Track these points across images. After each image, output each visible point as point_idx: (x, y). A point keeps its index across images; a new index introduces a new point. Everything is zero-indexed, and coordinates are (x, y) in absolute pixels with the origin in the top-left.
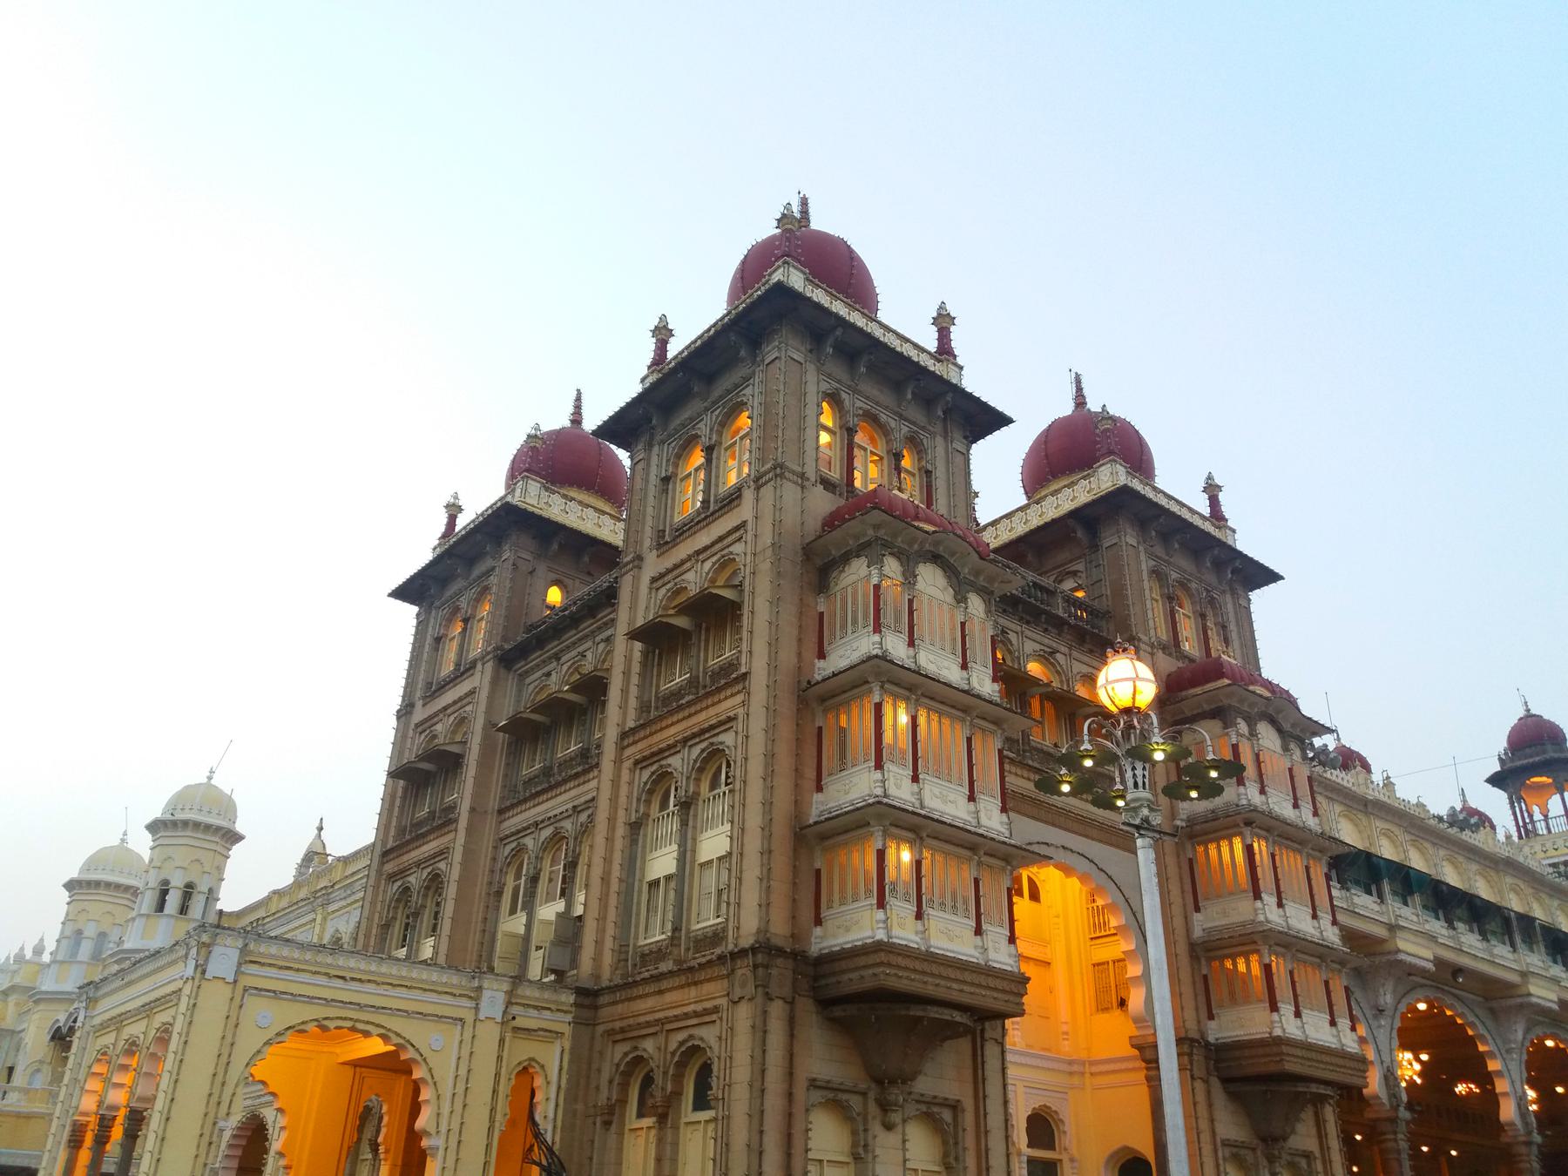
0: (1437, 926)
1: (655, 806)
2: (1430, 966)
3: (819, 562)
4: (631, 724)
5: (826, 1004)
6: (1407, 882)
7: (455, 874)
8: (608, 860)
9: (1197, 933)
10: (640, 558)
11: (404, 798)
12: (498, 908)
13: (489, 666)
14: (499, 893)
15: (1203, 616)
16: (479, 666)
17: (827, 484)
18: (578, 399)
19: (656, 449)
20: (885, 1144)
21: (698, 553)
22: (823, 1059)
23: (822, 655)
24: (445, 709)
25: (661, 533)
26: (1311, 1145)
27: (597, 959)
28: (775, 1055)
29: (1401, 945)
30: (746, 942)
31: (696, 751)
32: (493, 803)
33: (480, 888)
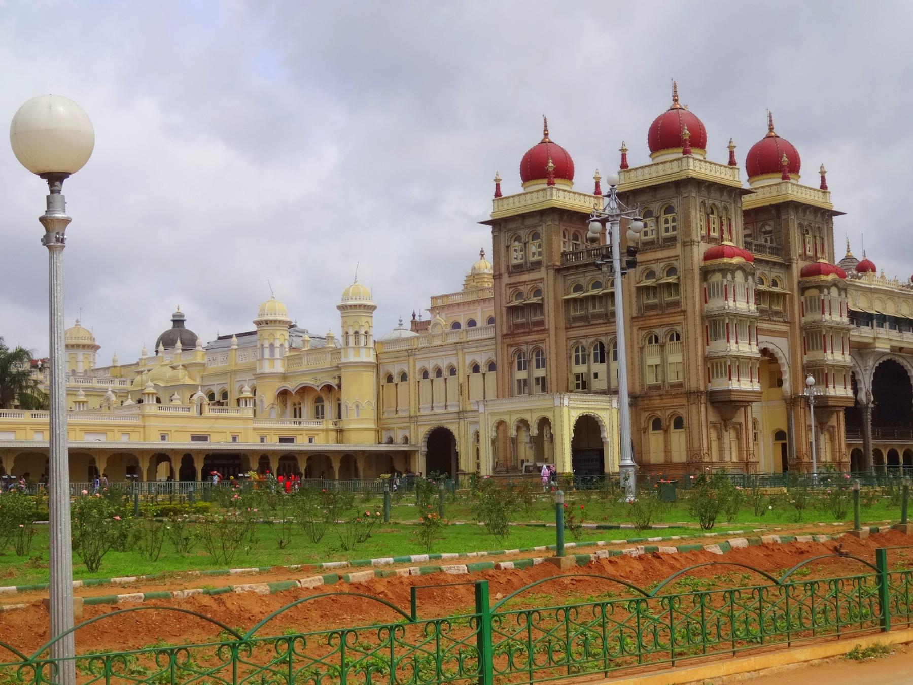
0: (894, 334)
1: (647, 342)
2: (888, 351)
4: (635, 314)
5: (712, 403)
6: (882, 319)
7: (553, 351)
9: (805, 362)
11: (507, 314)
13: (551, 272)
14: (570, 357)
15: (815, 237)
16: (543, 269)
17: (703, 237)
18: (545, 122)
20: (726, 435)
22: (713, 417)
23: (706, 303)
26: (835, 423)
28: (703, 418)
29: (878, 345)
30: (695, 389)
32: (562, 325)
33: (563, 355)
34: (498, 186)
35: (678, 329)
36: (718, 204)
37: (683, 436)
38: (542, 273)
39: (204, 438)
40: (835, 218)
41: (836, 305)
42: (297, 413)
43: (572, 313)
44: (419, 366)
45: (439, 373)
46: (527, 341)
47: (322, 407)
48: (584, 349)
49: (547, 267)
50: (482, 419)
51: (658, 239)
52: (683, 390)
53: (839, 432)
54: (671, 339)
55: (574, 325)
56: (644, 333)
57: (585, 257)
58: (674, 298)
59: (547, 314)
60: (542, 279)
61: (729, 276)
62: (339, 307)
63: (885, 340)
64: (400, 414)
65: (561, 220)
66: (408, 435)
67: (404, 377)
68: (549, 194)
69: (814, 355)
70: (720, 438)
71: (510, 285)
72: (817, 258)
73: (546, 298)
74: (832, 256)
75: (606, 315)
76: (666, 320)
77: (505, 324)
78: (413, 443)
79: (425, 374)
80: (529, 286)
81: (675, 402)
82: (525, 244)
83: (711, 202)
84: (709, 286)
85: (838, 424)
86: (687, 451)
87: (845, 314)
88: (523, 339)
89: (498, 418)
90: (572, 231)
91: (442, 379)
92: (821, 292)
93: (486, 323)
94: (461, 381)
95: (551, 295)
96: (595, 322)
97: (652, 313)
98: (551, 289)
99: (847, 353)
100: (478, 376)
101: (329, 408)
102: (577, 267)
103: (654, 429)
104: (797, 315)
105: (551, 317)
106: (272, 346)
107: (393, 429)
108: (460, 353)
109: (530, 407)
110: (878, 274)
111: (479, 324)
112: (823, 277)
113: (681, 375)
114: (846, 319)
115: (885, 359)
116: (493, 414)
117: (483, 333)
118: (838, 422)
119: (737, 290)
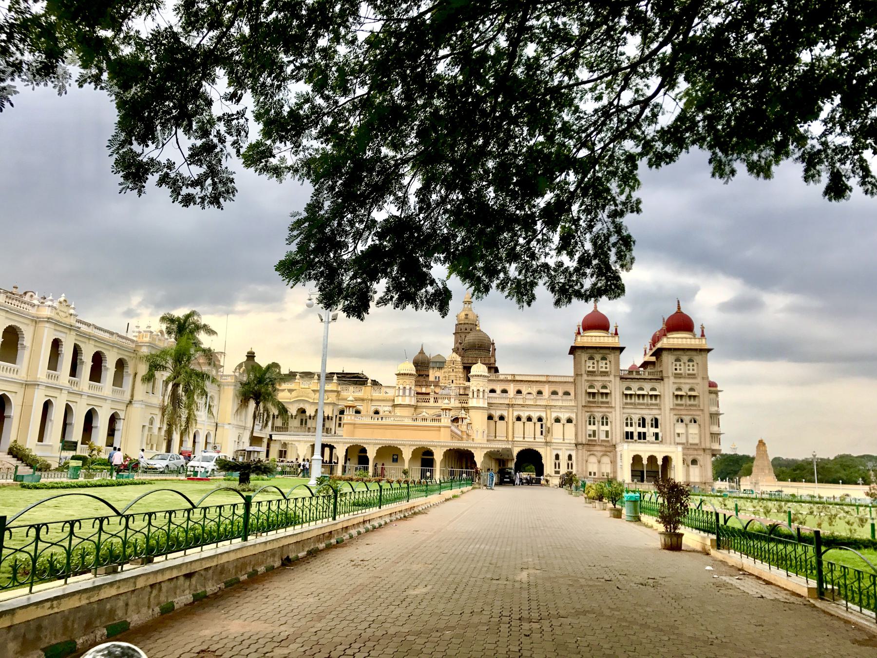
35: (697, 418)
38: (611, 378)
44: (516, 414)
45: (529, 419)
48: (631, 419)
49: (615, 376)
54: (691, 421)
64: (498, 438)
67: (502, 418)
71: (588, 381)
76: (691, 413)
81: (695, 452)
88: (596, 409)
89: (635, 453)
105: (616, 399)
108: (548, 411)
116: (632, 451)
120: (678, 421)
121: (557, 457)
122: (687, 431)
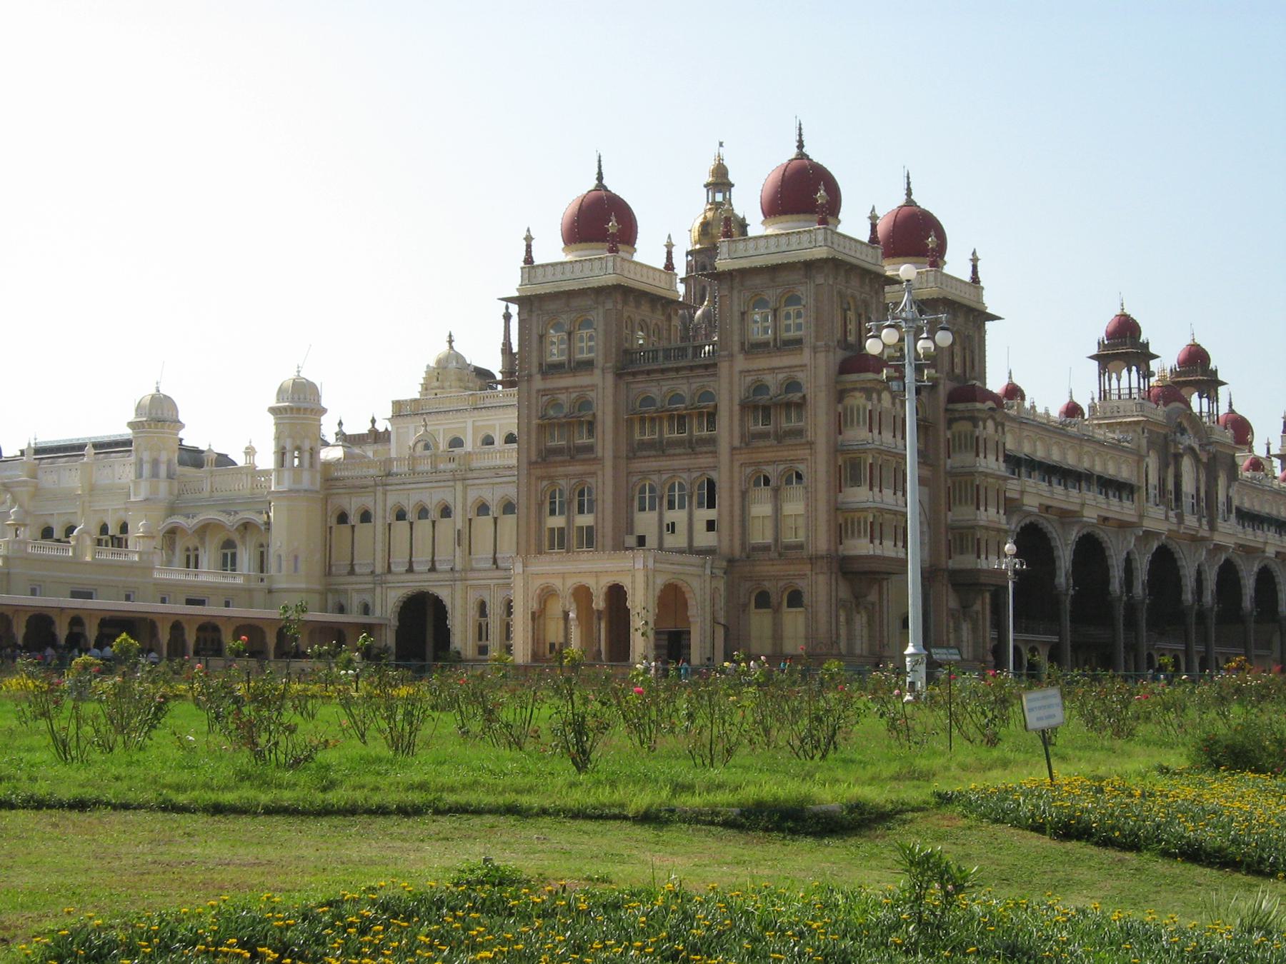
0: (1044, 485)
2: (1036, 510)
3: (839, 387)
8: (732, 506)
9: (949, 521)
10: (731, 356)
12: (632, 506)
13: (610, 378)
14: (633, 500)
16: (598, 372)
19: (735, 293)
21: (773, 369)
22: (844, 592)
23: (840, 433)
24: (567, 388)
25: (743, 344)
27: (731, 547)
29: (1027, 500)
30: (824, 553)
31: (782, 467)
34: (529, 247)
35: (801, 468)
36: (857, 294)
37: (801, 620)
38: (595, 378)
39: (88, 595)
40: (989, 325)
41: (991, 445)
42: (192, 561)
43: (637, 437)
45: (423, 513)
46: (566, 476)
47: (234, 556)
49: (603, 370)
50: (518, 583)
51: (775, 340)
52: (804, 554)
53: (984, 619)
54: (789, 482)
55: (639, 454)
56: (749, 470)
57: (661, 359)
58: (794, 424)
59: (600, 437)
60: (593, 387)
61: (875, 396)
62: (273, 410)
63: (1035, 494)
65: (625, 302)
66: (367, 598)
67: (366, 517)
68: (610, 264)
69: (962, 513)
70: (849, 621)
71: (544, 392)
72: (966, 380)
73: (599, 414)
74: (982, 376)
75: (690, 442)
76: (785, 454)
77: (533, 449)
78: (378, 613)
79: (401, 516)
80: (574, 395)
82: (570, 334)
83: (849, 291)
84: (845, 409)
85: (983, 609)
86: (806, 638)
87: (1001, 459)
88: (561, 470)
90: (637, 319)
91: (426, 524)
92: (975, 426)
93: (479, 443)
94: (459, 526)
95: (609, 409)
96: (672, 451)
97: (761, 443)
98: (610, 399)
99: (1002, 512)
100: (487, 521)
101: (245, 558)
102: (649, 372)
103: (756, 607)
104: (942, 456)
105: (605, 442)
106: (155, 463)
107: (345, 591)
108: (459, 486)
109: (597, 570)
110: (1027, 404)
111: (468, 446)
112: (979, 405)
113: (802, 533)
114: (1003, 466)
115: (1027, 521)
117: (508, 456)
118: (982, 606)
119: (883, 419)
120: (757, 484)
121: (482, 607)
122: (777, 510)
